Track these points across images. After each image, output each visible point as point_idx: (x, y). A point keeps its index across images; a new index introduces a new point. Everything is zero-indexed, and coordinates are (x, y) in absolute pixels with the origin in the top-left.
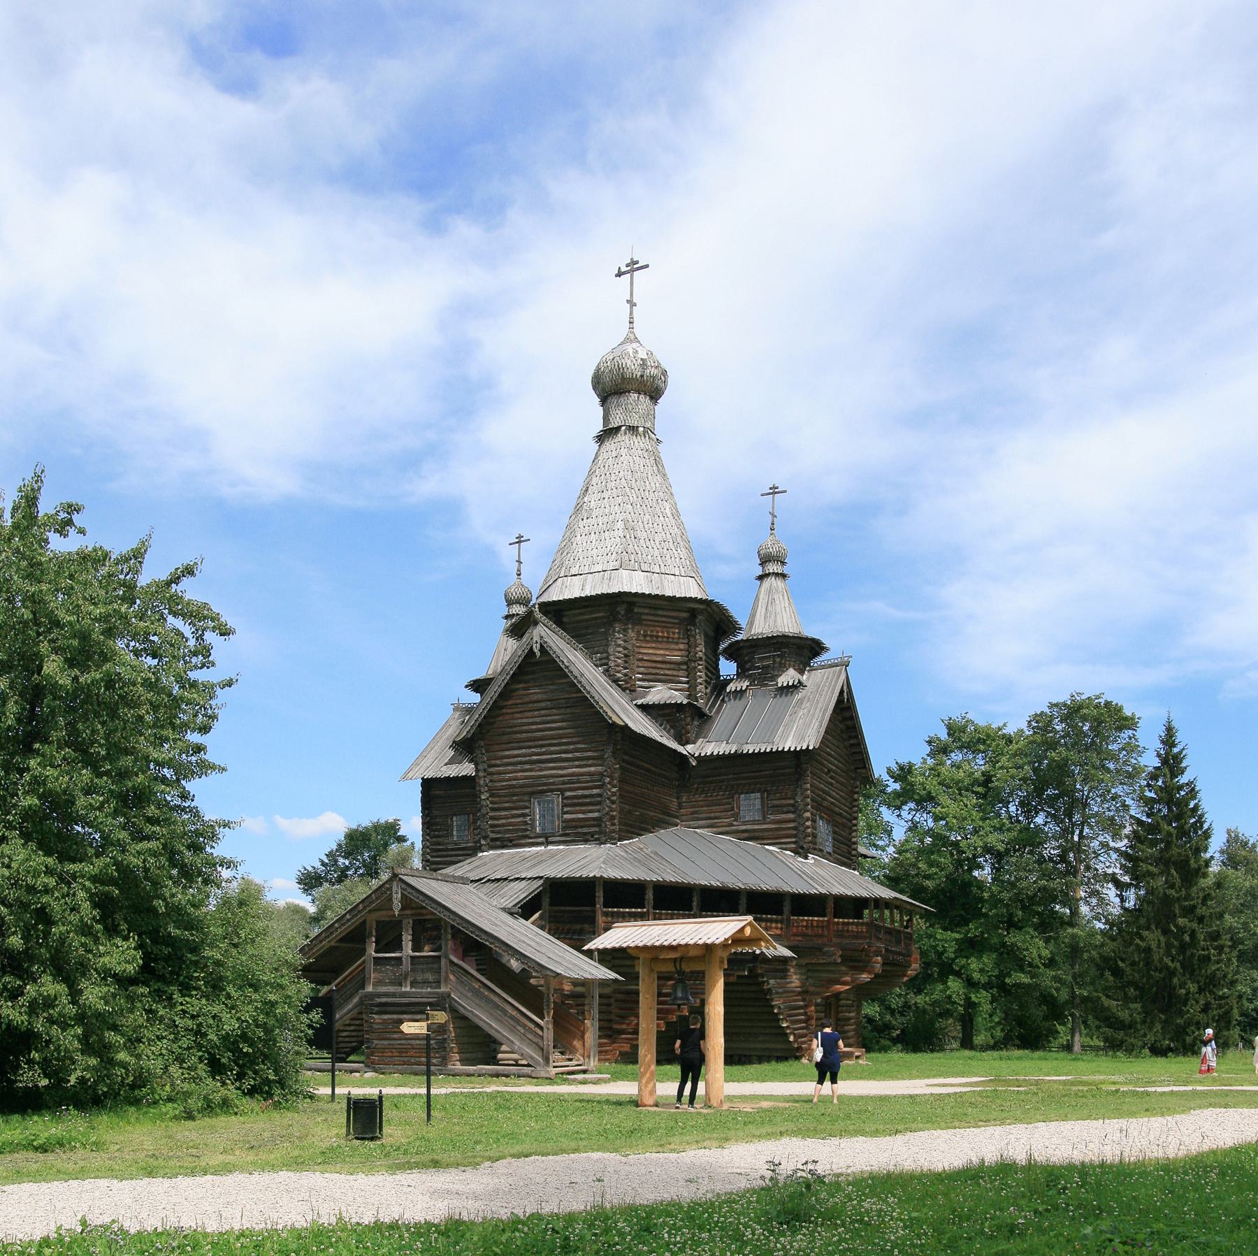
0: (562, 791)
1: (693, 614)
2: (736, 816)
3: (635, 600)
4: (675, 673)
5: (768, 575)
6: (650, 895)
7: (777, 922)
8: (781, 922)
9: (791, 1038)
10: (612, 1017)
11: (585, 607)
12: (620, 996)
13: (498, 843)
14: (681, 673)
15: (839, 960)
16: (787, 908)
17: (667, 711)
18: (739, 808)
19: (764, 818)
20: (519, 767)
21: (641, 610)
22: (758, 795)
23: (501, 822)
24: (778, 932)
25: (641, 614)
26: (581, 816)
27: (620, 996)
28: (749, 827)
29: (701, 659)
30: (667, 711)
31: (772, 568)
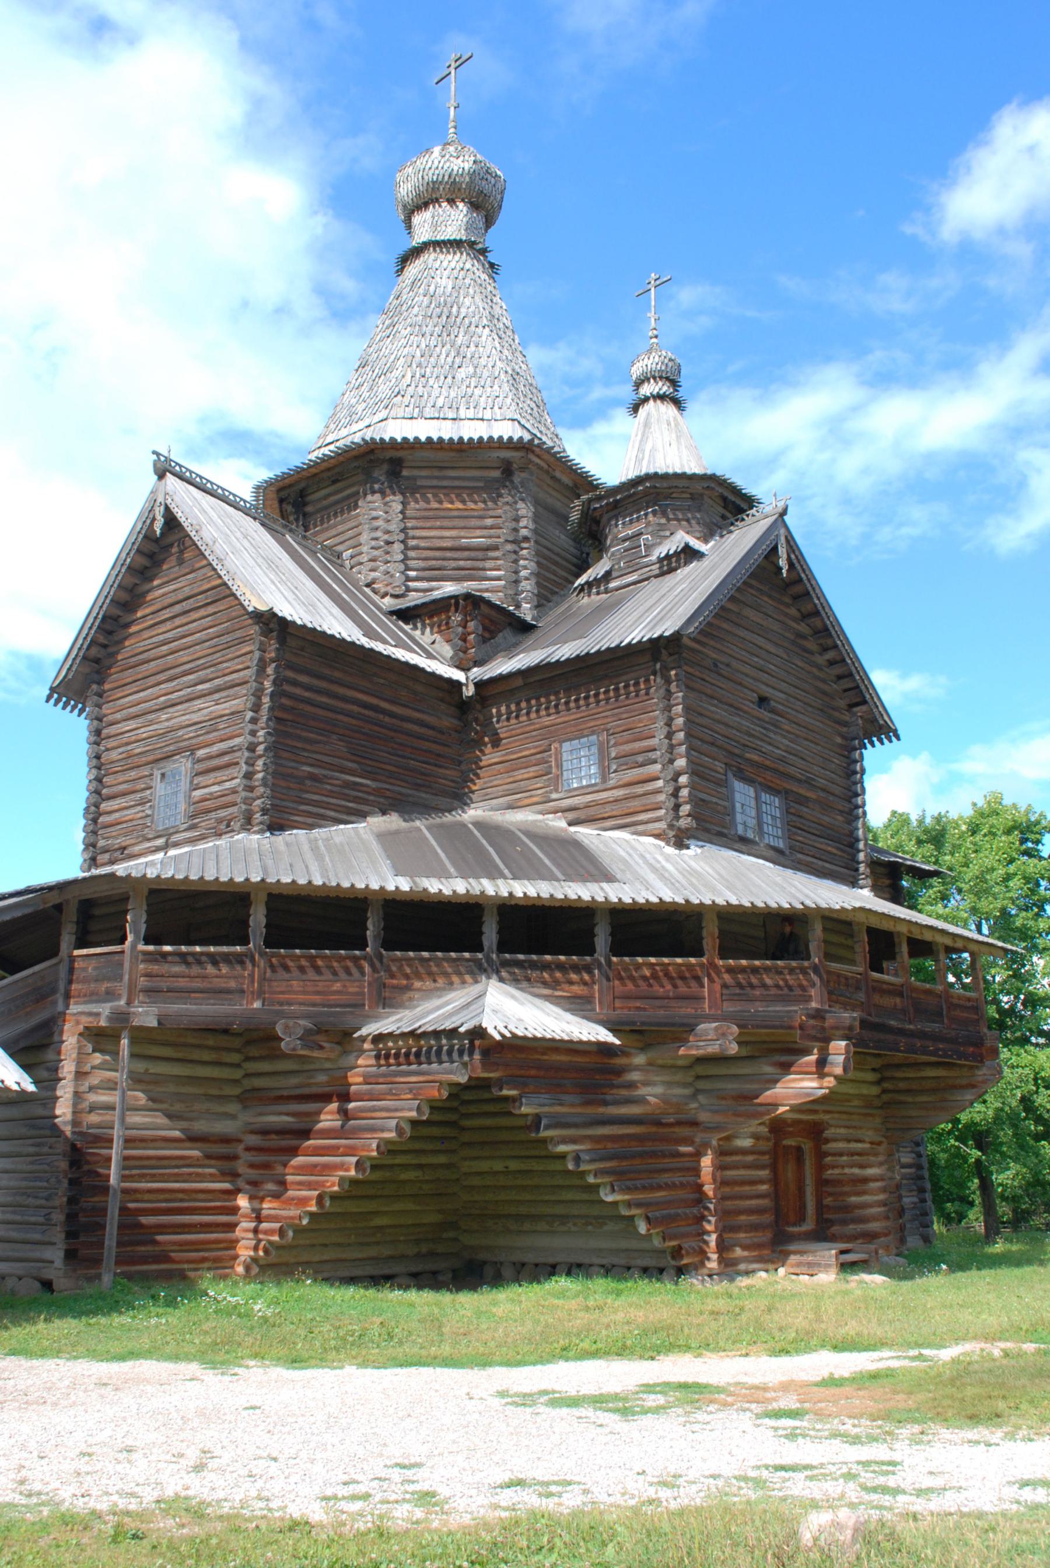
1: (508, 470)
2: (556, 782)
4: (480, 564)
5: (646, 400)
6: (258, 918)
7: (576, 968)
8: (588, 969)
9: (642, 1228)
11: (334, 482)
12: (253, 1140)
14: (489, 564)
15: (733, 1049)
16: (602, 940)
18: (559, 766)
19: (604, 778)
21: (416, 473)
24: (576, 989)
25: (414, 478)
26: (215, 788)
27: (253, 1140)
29: (526, 539)
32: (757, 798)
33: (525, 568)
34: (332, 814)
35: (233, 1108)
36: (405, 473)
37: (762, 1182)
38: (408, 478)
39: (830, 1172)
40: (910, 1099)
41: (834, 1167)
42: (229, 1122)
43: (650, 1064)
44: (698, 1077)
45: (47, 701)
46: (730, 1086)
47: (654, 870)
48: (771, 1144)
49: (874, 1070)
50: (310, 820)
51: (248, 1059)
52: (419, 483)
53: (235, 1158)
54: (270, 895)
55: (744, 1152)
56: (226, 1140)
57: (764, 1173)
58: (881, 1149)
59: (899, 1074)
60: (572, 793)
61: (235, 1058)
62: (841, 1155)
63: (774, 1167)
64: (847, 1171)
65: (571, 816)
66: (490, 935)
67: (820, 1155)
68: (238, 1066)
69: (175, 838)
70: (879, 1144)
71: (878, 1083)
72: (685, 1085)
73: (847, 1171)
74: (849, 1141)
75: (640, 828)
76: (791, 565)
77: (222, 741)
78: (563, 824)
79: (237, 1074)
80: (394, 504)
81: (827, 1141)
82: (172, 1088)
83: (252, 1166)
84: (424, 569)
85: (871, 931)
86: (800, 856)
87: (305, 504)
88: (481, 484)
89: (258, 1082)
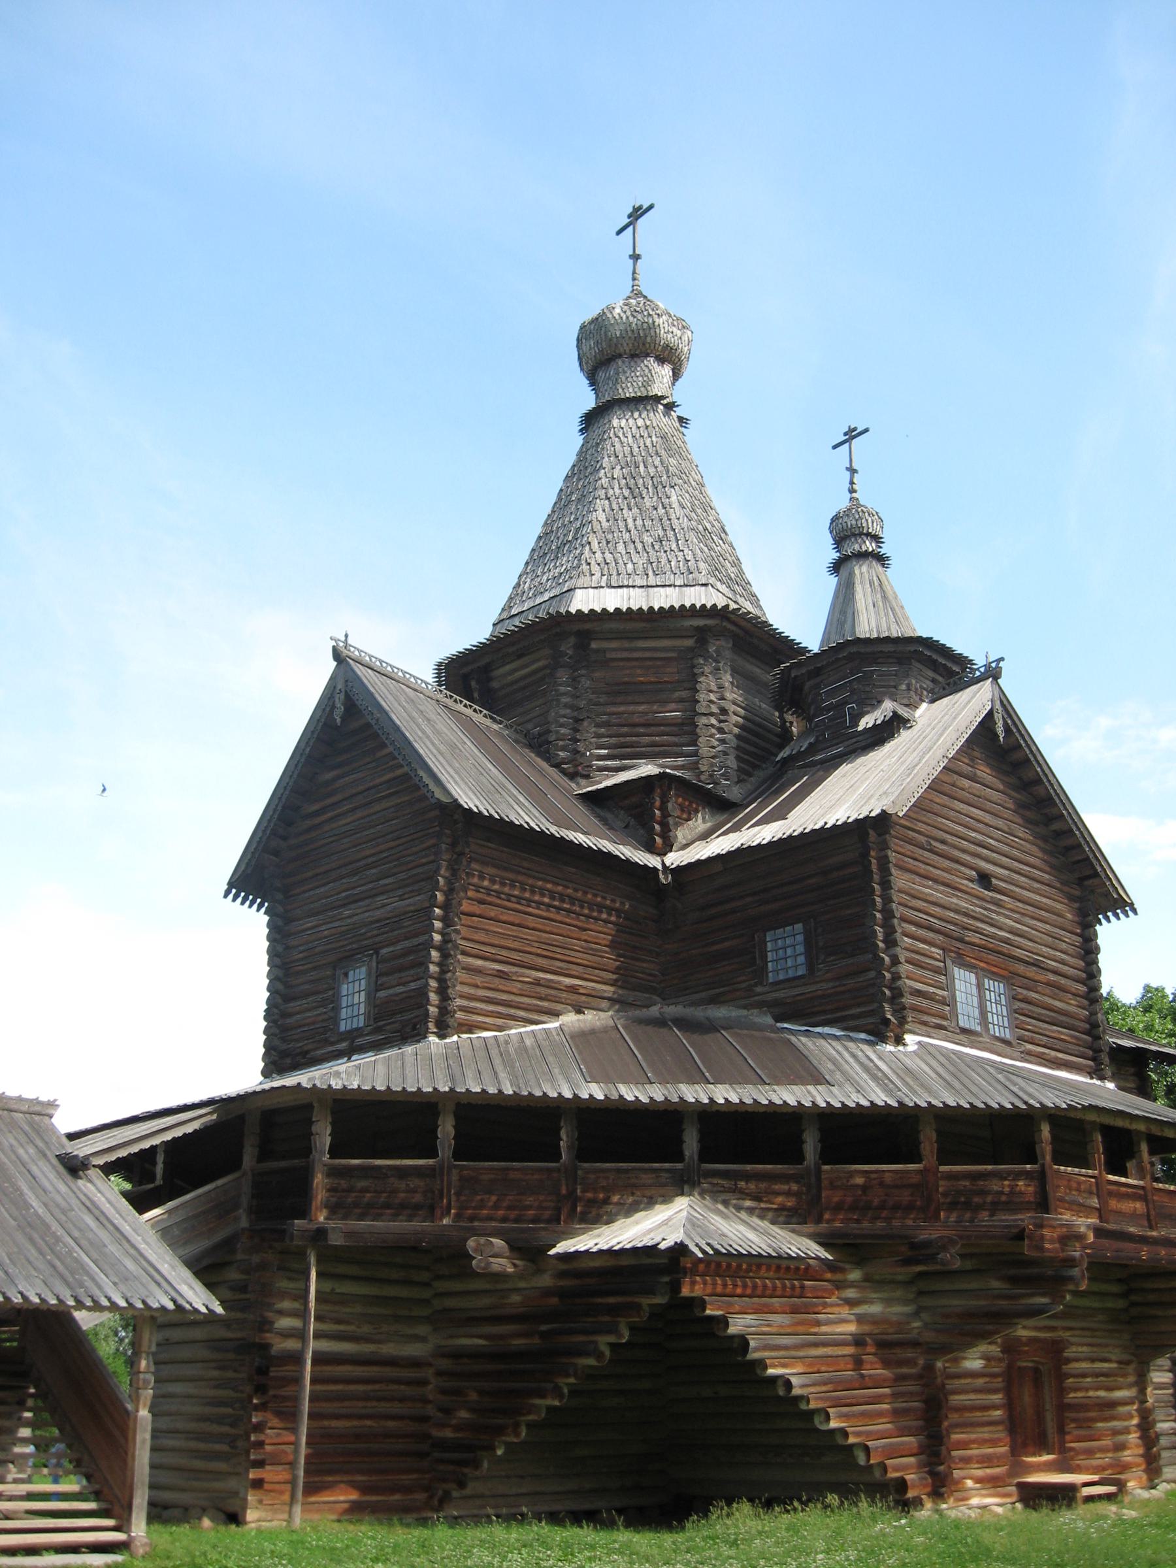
2: (761, 973)
6: (446, 1129)
10: (430, 1410)
11: (520, 656)
12: (444, 1364)
22: (799, 927)
25: (604, 651)
27: (444, 1364)
31: (855, 547)
32: (980, 986)
34: (522, 1014)
35: (422, 1330)
36: (594, 645)
37: (995, 1407)
38: (597, 651)
39: (1071, 1395)
40: (1160, 1313)
41: (1076, 1390)
42: (419, 1346)
43: (867, 1279)
44: (921, 1293)
45: (226, 896)
46: (955, 1302)
47: (866, 1069)
48: (1004, 1365)
49: (1120, 1281)
50: (500, 1022)
51: (439, 1277)
52: (608, 656)
53: (423, 1383)
54: (458, 1105)
55: (973, 1375)
56: (415, 1363)
57: (997, 1398)
58: (1131, 1369)
59: (1149, 1285)
61: (425, 1276)
62: (1084, 1376)
63: (1008, 1391)
64: (1091, 1394)
66: (691, 1143)
67: (1061, 1377)
68: (427, 1285)
69: (359, 1041)
70: (1128, 1363)
71: (1124, 1295)
72: (906, 1302)
73: (1091, 1394)
74: (1093, 1360)
75: (852, 1023)
76: (1007, 730)
77: (407, 939)
79: (426, 1294)
80: (583, 679)
81: (1068, 1361)
82: (358, 1309)
83: (444, 1392)
84: (616, 746)
85: (1107, 1130)
86: (1030, 1046)
87: (490, 679)
88: (674, 655)
89: (450, 1303)
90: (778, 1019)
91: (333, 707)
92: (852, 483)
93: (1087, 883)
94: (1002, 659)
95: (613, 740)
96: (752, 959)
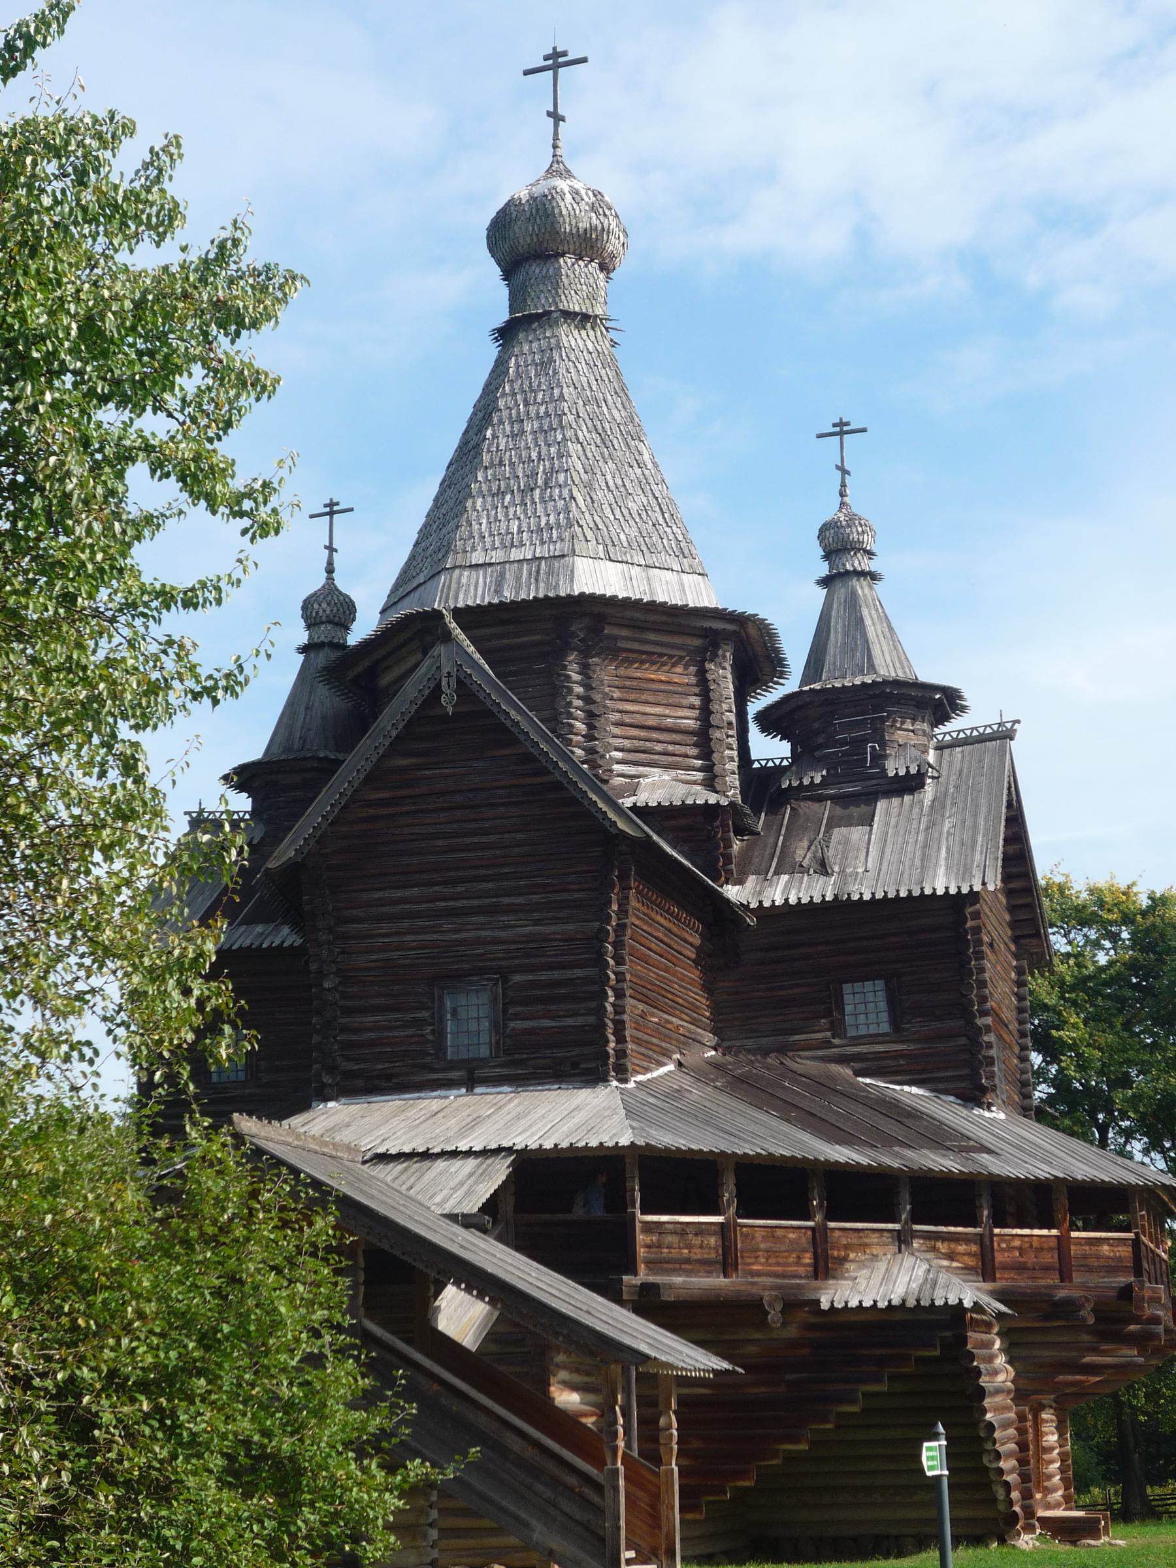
0: (504, 975)
2: (838, 1027)
3: (608, 611)
13: (360, 1083)
17: (683, 822)
20: (406, 924)
21: (616, 631)
23: (365, 1036)
25: (616, 638)
28: (864, 1049)
30: (683, 822)
33: (732, 759)
38: (609, 637)
46: (1047, 1353)
54: (737, 1163)
60: (857, 1040)
65: (857, 1065)
69: (479, 1073)
75: (941, 1086)
78: (849, 1072)
84: (629, 751)
90: (858, 1073)
91: (437, 690)
92: (843, 485)
93: (1022, 941)
94: (1018, 722)
95: (627, 743)
96: (830, 1009)
